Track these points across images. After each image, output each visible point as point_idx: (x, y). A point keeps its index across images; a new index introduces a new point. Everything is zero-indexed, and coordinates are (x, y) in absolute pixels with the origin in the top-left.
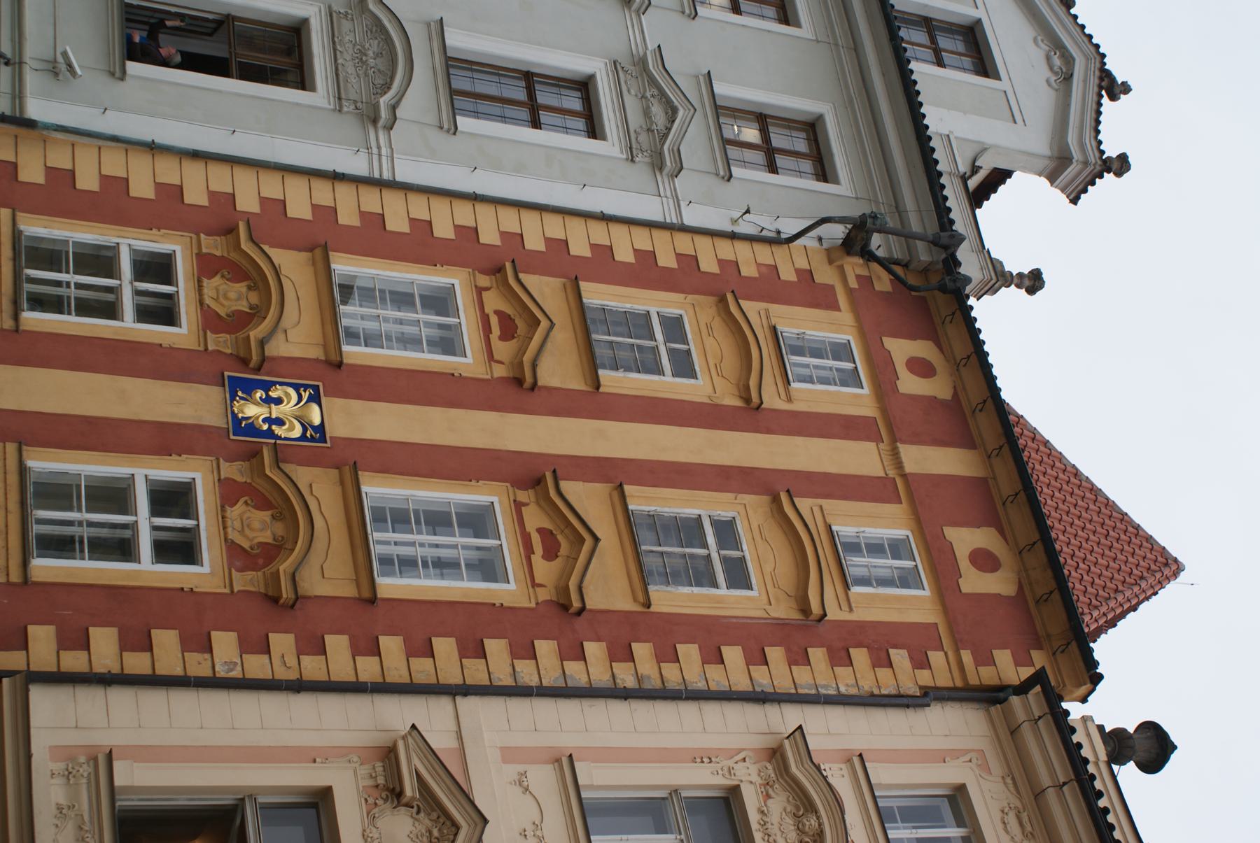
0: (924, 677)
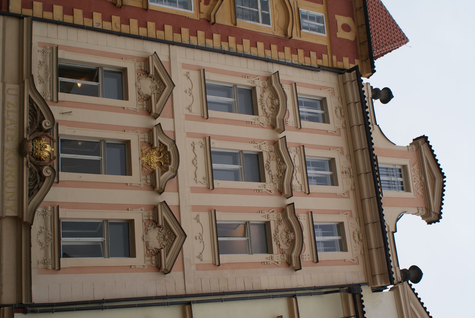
0: (320, 62)
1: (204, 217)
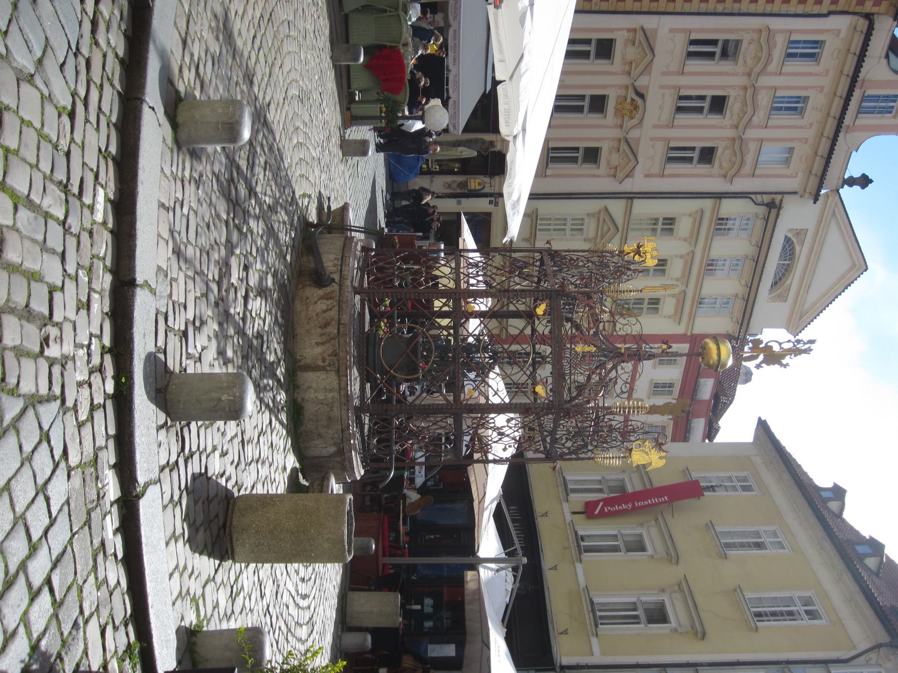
0: (833, 8)
1: (660, 148)
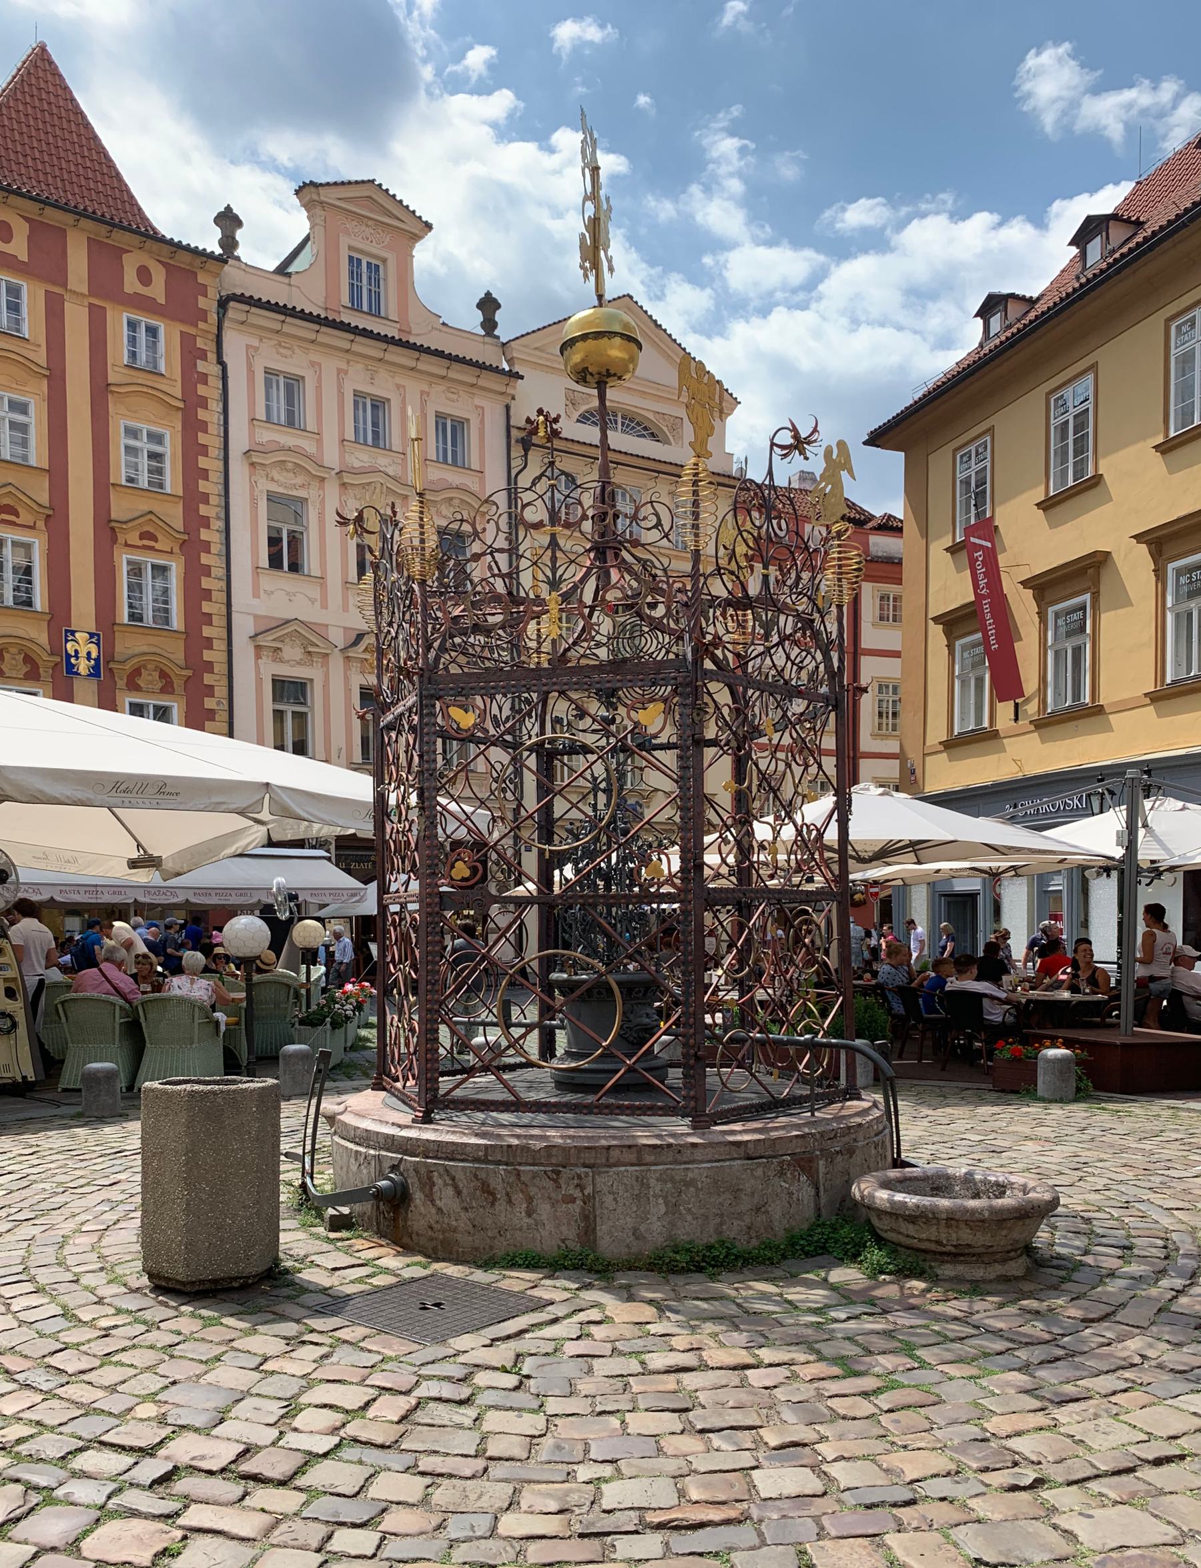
0: (212, 357)
